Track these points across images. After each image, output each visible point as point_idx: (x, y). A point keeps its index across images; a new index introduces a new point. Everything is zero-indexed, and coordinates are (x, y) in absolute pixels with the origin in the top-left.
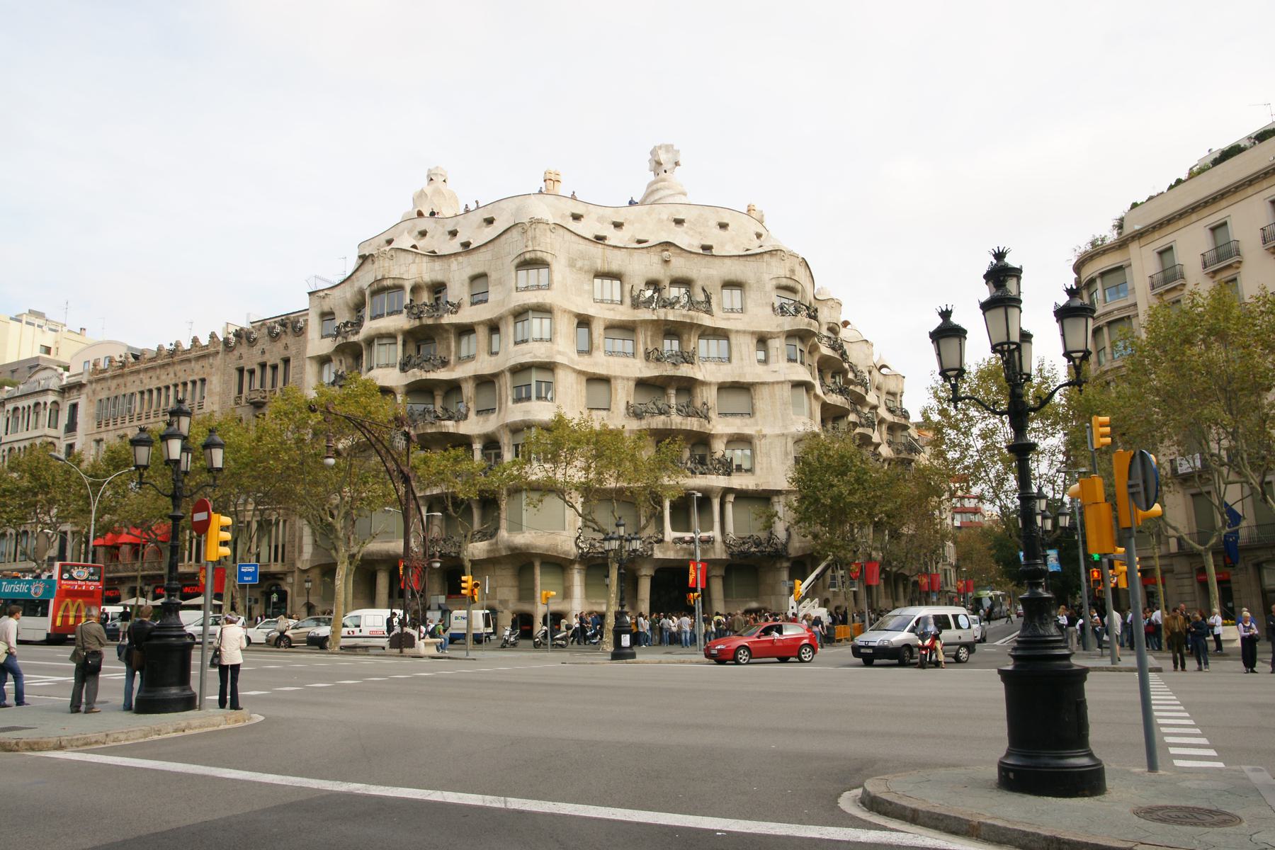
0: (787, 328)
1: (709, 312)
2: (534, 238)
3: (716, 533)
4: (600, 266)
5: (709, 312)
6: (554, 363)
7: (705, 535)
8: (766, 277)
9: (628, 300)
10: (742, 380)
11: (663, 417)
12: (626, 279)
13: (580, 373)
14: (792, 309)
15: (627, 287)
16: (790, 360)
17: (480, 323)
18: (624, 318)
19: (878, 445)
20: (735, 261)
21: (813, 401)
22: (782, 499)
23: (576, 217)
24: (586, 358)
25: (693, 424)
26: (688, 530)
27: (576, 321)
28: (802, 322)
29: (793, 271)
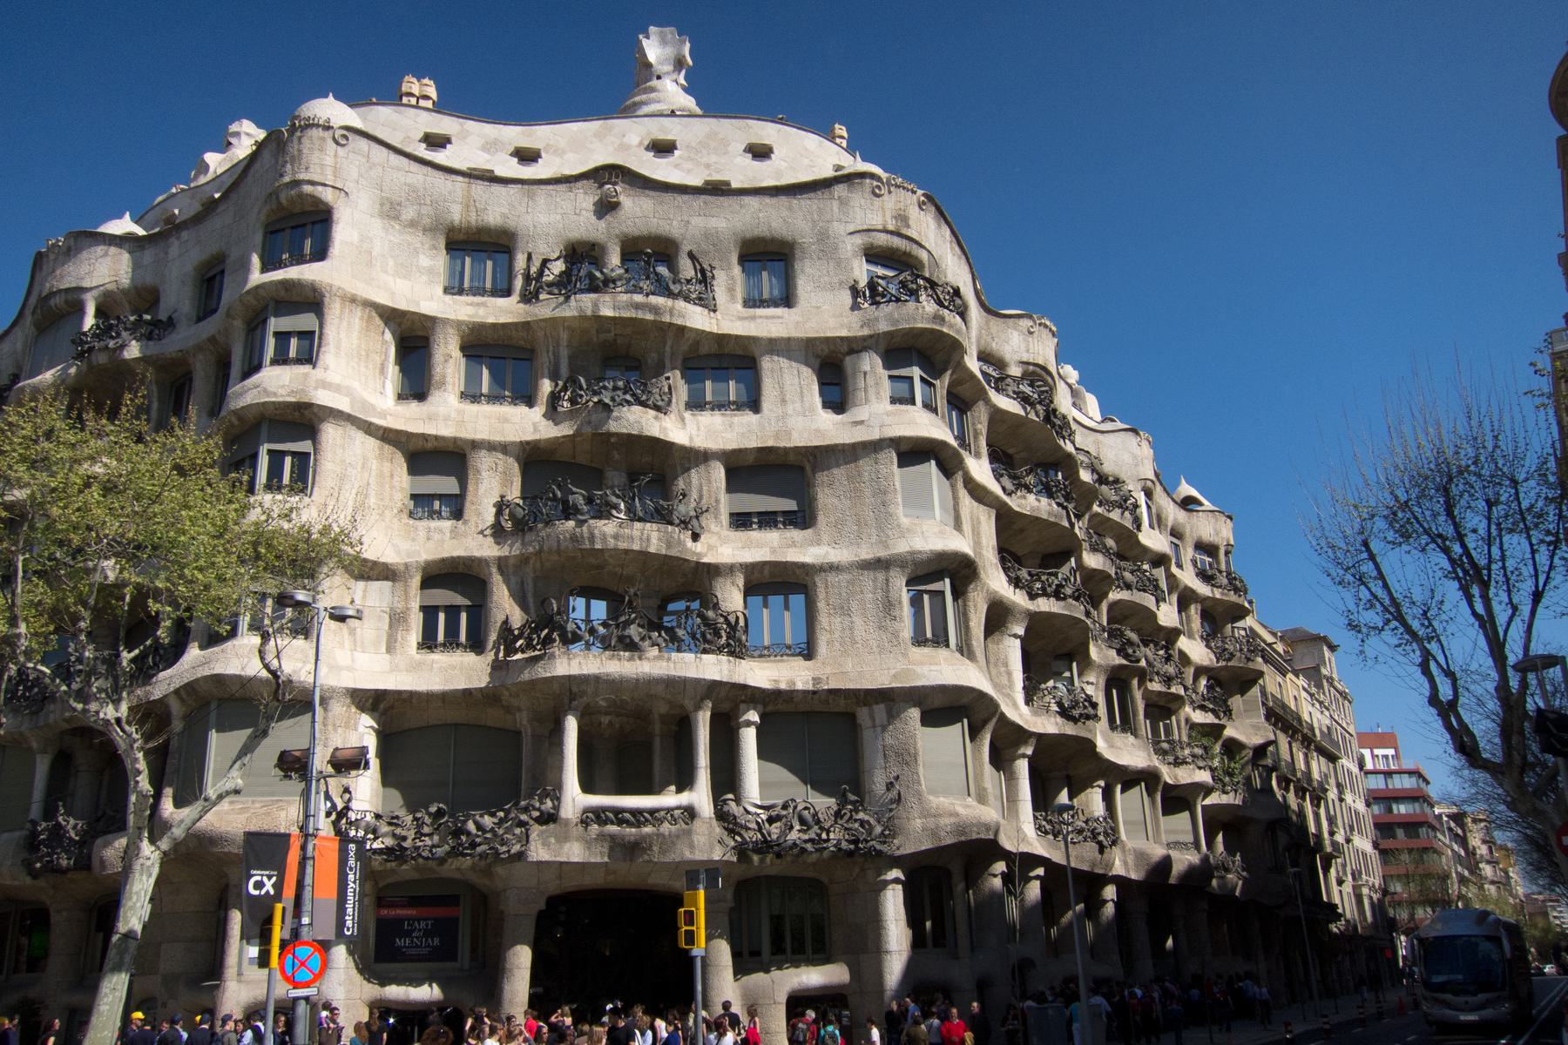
0: (883, 327)
2: (296, 159)
3: (700, 796)
4: (456, 215)
6: (310, 405)
8: (839, 229)
9: (519, 283)
10: (782, 444)
12: (521, 244)
16: (894, 401)
17: (199, 348)
18: (502, 320)
19: (1174, 634)
21: (966, 501)
22: (880, 710)
23: (436, 141)
24: (414, 407)
28: (922, 312)
29: (902, 218)
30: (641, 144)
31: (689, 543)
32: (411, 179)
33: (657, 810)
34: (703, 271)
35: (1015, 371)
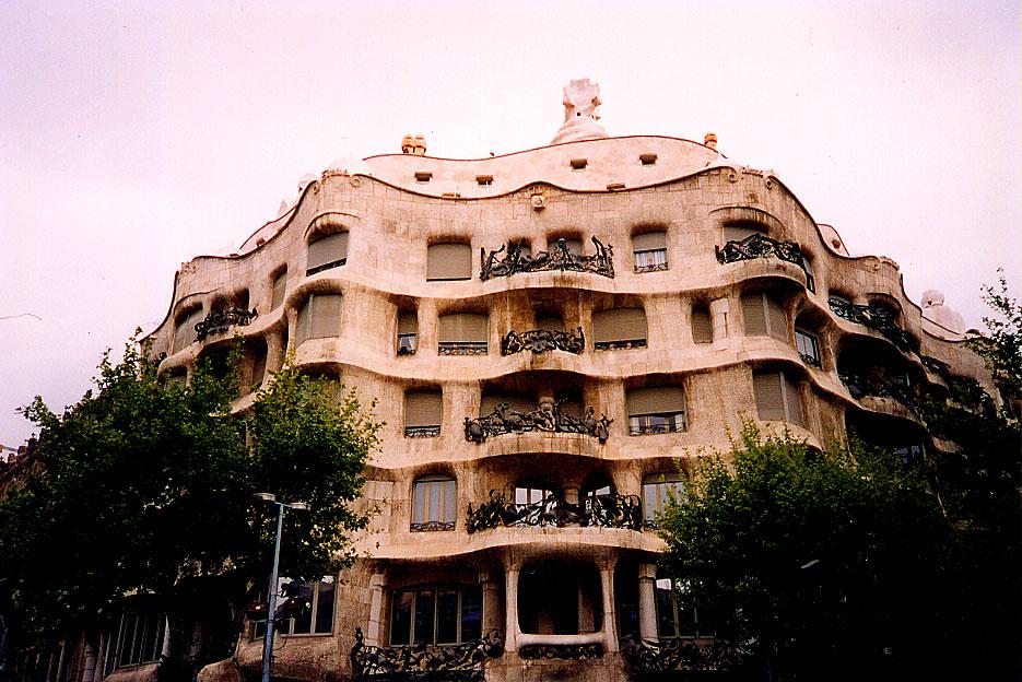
1: (607, 271)
3: (609, 635)
5: (607, 271)
7: (583, 639)
11: (513, 435)
13: (389, 380)
14: (745, 248)
15: (476, 254)
17: (269, 331)
20: (650, 194)
21: (816, 407)
23: (423, 178)
24: (406, 361)
25: (562, 442)
26: (576, 632)
27: (392, 308)
28: (766, 265)
30: (563, 164)
31: (597, 446)
32: (401, 205)
33: (574, 647)
34: (603, 249)
35: (863, 302)
